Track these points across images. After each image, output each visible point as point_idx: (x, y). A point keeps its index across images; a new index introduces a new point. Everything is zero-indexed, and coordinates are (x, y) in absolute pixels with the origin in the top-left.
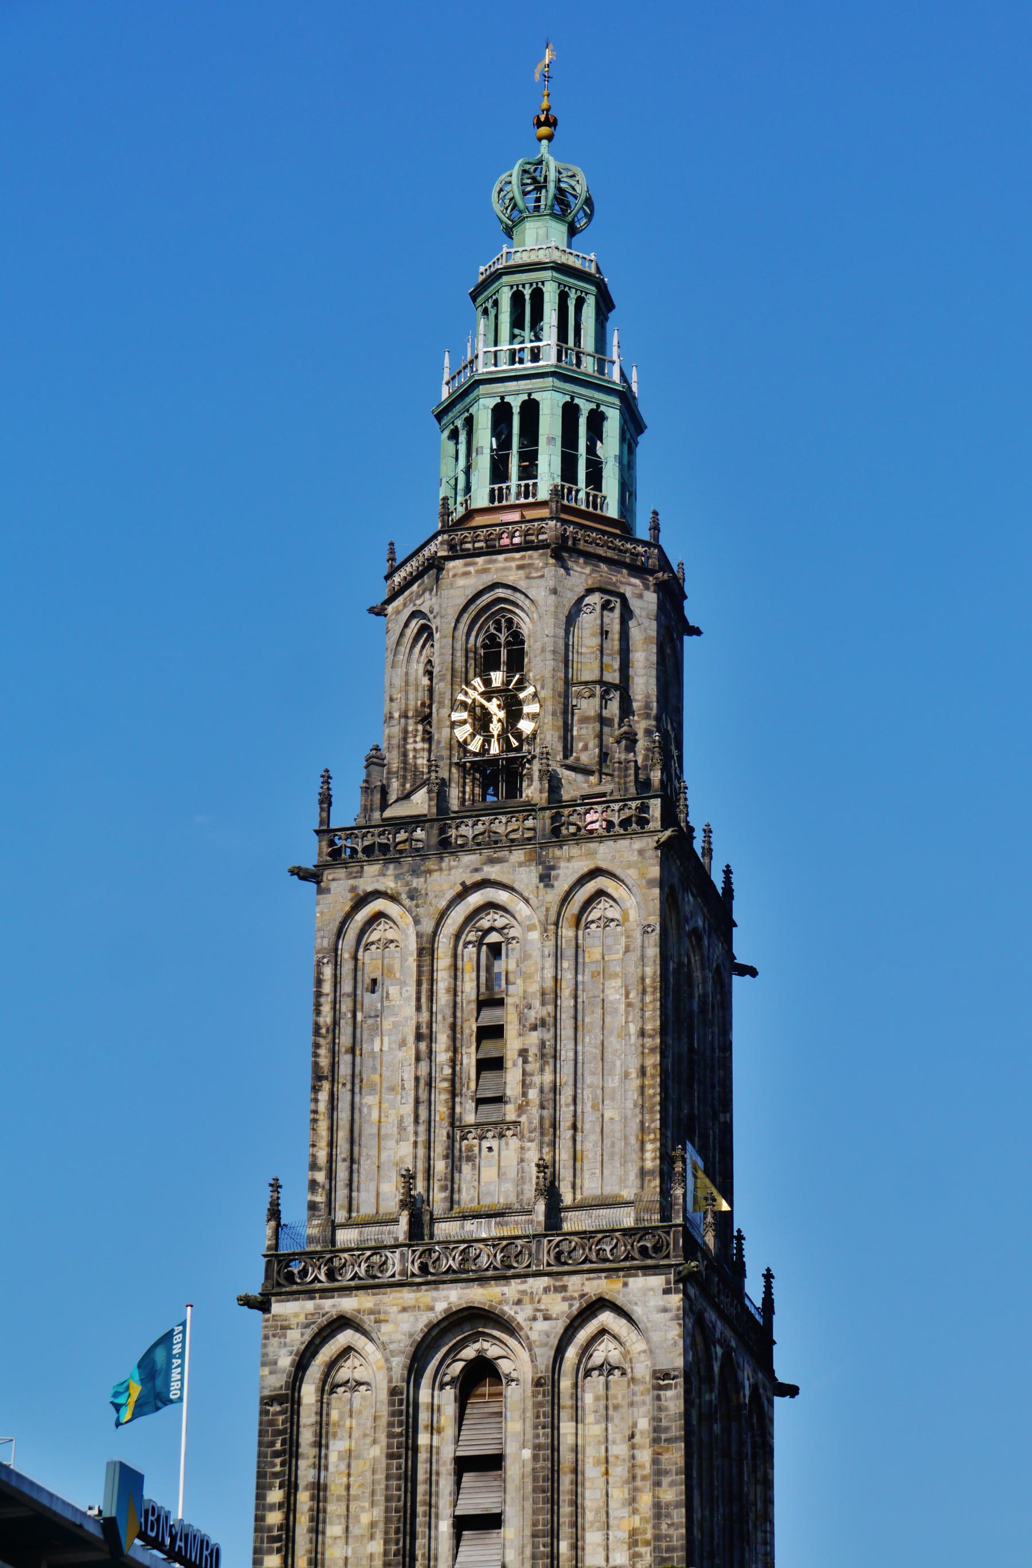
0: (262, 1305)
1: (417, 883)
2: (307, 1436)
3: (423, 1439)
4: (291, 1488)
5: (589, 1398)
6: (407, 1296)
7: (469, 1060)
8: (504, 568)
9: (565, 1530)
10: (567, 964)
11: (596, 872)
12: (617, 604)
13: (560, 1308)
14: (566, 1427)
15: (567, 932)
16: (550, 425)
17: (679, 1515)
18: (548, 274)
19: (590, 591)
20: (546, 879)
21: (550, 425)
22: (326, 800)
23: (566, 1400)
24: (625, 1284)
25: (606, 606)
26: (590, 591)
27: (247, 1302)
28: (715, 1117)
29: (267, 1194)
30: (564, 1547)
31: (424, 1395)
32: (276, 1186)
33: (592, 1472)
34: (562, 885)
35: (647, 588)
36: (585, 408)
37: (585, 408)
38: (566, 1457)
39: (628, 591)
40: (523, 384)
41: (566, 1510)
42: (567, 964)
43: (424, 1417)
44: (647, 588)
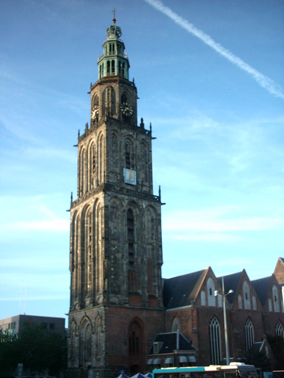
0: (70, 211)
1: (86, 142)
2: (75, 228)
3: (86, 225)
4: (73, 236)
5: (100, 214)
6: (81, 205)
7: (92, 166)
8: (96, 90)
9: (96, 235)
10: (99, 147)
11: (101, 132)
12: (110, 88)
13: (93, 201)
14: (96, 219)
15: (99, 142)
16: (105, 65)
17: (104, 229)
18: (115, 42)
19: (106, 88)
20: (96, 135)
21: (116, 64)
22: (79, 134)
23: (96, 215)
24: (99, 195)
25: (108, 90)
26: (106, 88)
27: (67, 211)
28: (147, 163)
29: (71, 194)
30: (96, 237)
31: (86, 219)
32: (72, 193)
33: (100, 225)
34: (98, 135)
35: (117, 84)
36: (111, 60)
37: (111, 60)
38: (96, 223)
39: (113, 86)
40: (102, 61)
41: (96, 232)
42: (99, 147)
43: (86, 222)
44: (117, 84)
